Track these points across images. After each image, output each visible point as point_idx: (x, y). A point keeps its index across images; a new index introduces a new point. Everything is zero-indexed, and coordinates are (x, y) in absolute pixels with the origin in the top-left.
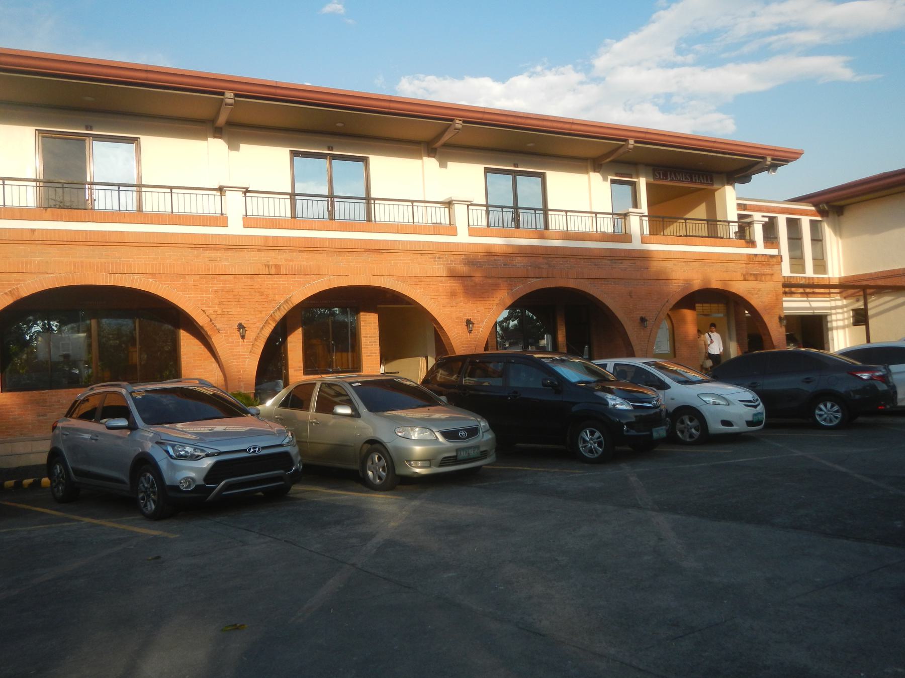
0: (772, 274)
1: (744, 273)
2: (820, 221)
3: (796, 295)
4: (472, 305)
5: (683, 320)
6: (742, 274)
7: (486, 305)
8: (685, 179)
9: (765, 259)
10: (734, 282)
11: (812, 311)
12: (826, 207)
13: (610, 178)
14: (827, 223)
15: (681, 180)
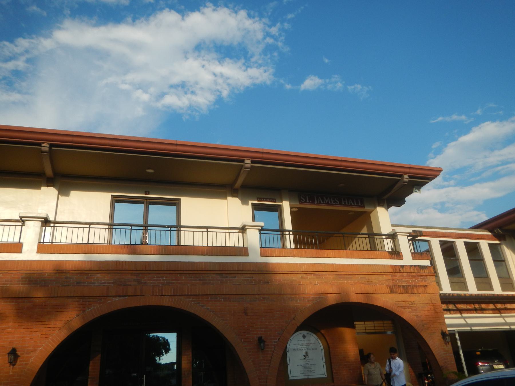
0: (426, 286)
1: (391, 285)
2: (499, 244)
3: (487, 312)
4: (23, 330)
5: (341, 340)
6: (387, 286)
7: (44, 330)
8: (334, 202)
9: (414, 270)
10: (379, 295)
11: (508, 327)
12: (500, 231)
13: (251, 202)
14: (505, 245)
15: (330, 203)
